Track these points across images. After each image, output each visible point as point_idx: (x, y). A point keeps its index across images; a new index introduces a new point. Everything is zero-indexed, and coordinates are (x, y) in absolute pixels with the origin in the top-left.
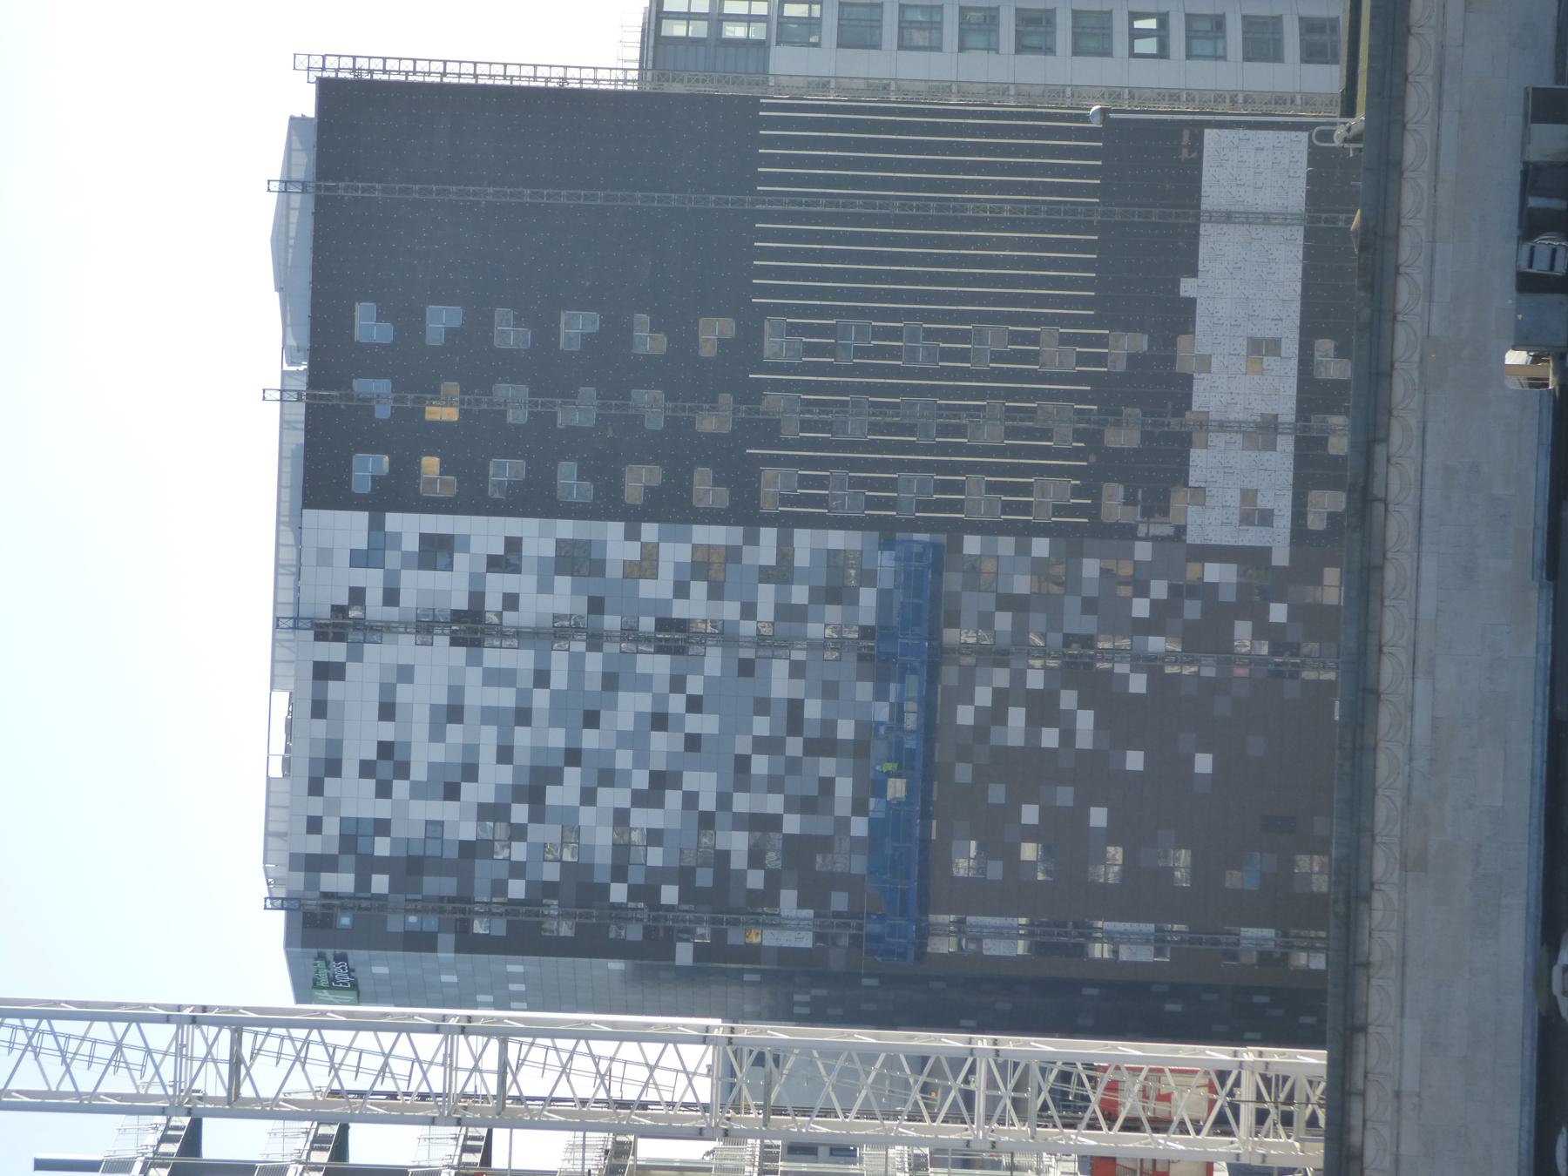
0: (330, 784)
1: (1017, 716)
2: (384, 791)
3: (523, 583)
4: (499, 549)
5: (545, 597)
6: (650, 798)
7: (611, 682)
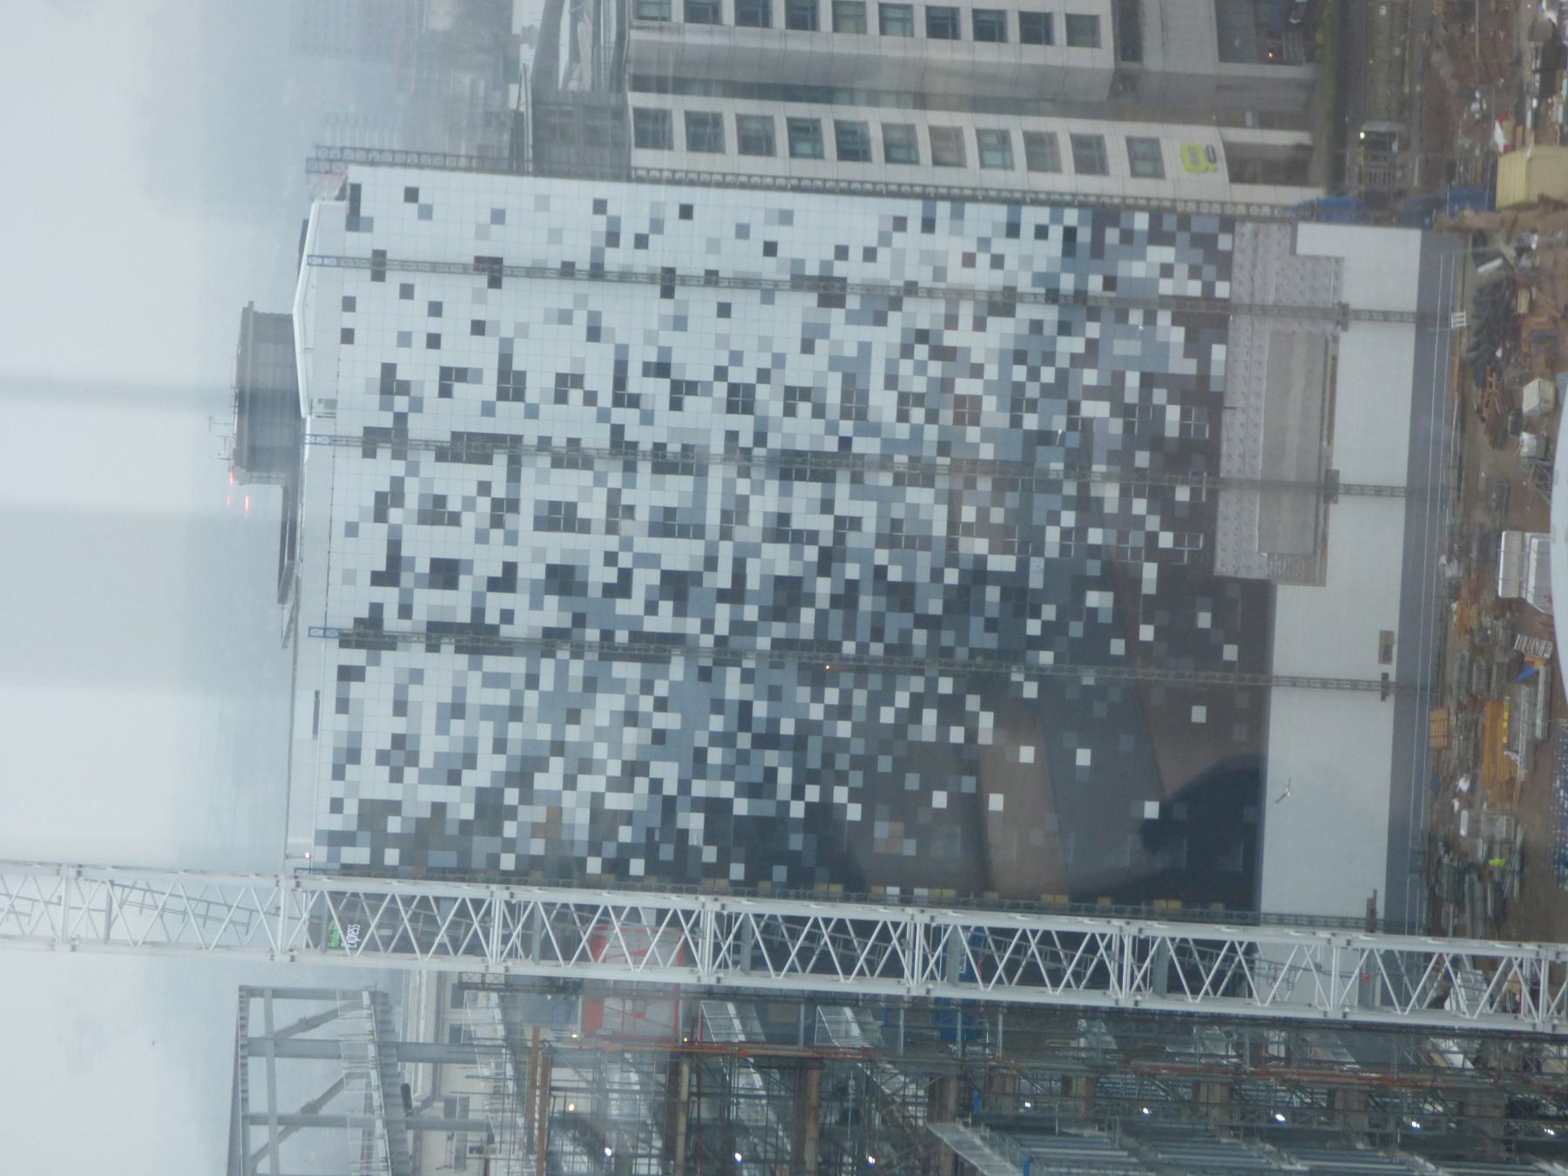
0: (350, 769)
1: (930, 716)
2: (396, 776)
3: (517, 601)
4: (498, 573)
5: (536, 613)
6: (623, 783)
7: (590, 685)
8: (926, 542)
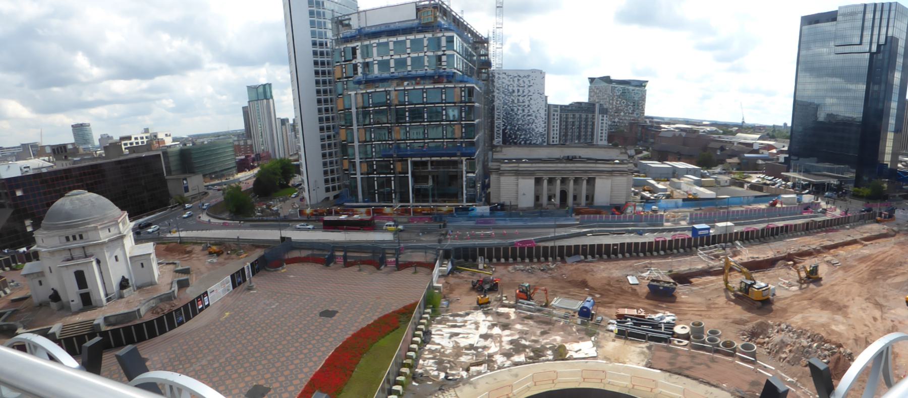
7: (505, 94)
8: (518, 122)
